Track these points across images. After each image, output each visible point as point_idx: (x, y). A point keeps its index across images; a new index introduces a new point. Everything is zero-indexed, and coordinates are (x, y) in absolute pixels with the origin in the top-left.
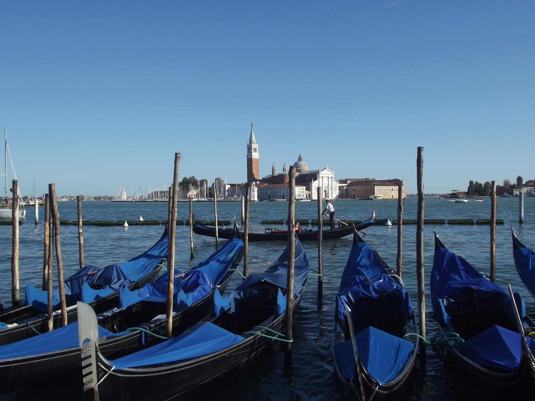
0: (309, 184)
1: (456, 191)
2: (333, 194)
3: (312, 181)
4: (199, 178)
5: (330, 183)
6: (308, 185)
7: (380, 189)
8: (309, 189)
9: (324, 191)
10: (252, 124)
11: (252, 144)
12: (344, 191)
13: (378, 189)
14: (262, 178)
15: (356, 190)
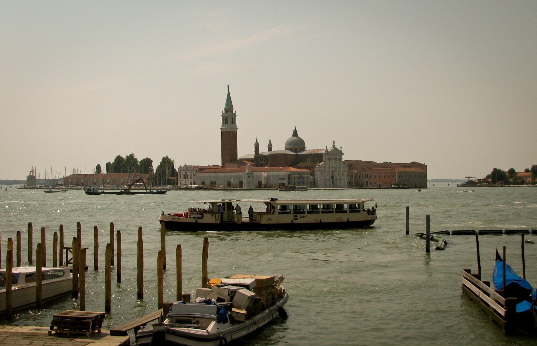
0: (314, 168)
1: (471, 177)
2: (342, 181)
3: (317, 163)
4: (139, 157)
5: (338, 166)
6: (313, 169)
7: (403, 175)
8: (313, 174)
9: (331, 177)
10: (228, 86)
11: (229, 112)
12: (354, 177)
13: (400, 174)
14: (240, 159)
15: (369, 177)
